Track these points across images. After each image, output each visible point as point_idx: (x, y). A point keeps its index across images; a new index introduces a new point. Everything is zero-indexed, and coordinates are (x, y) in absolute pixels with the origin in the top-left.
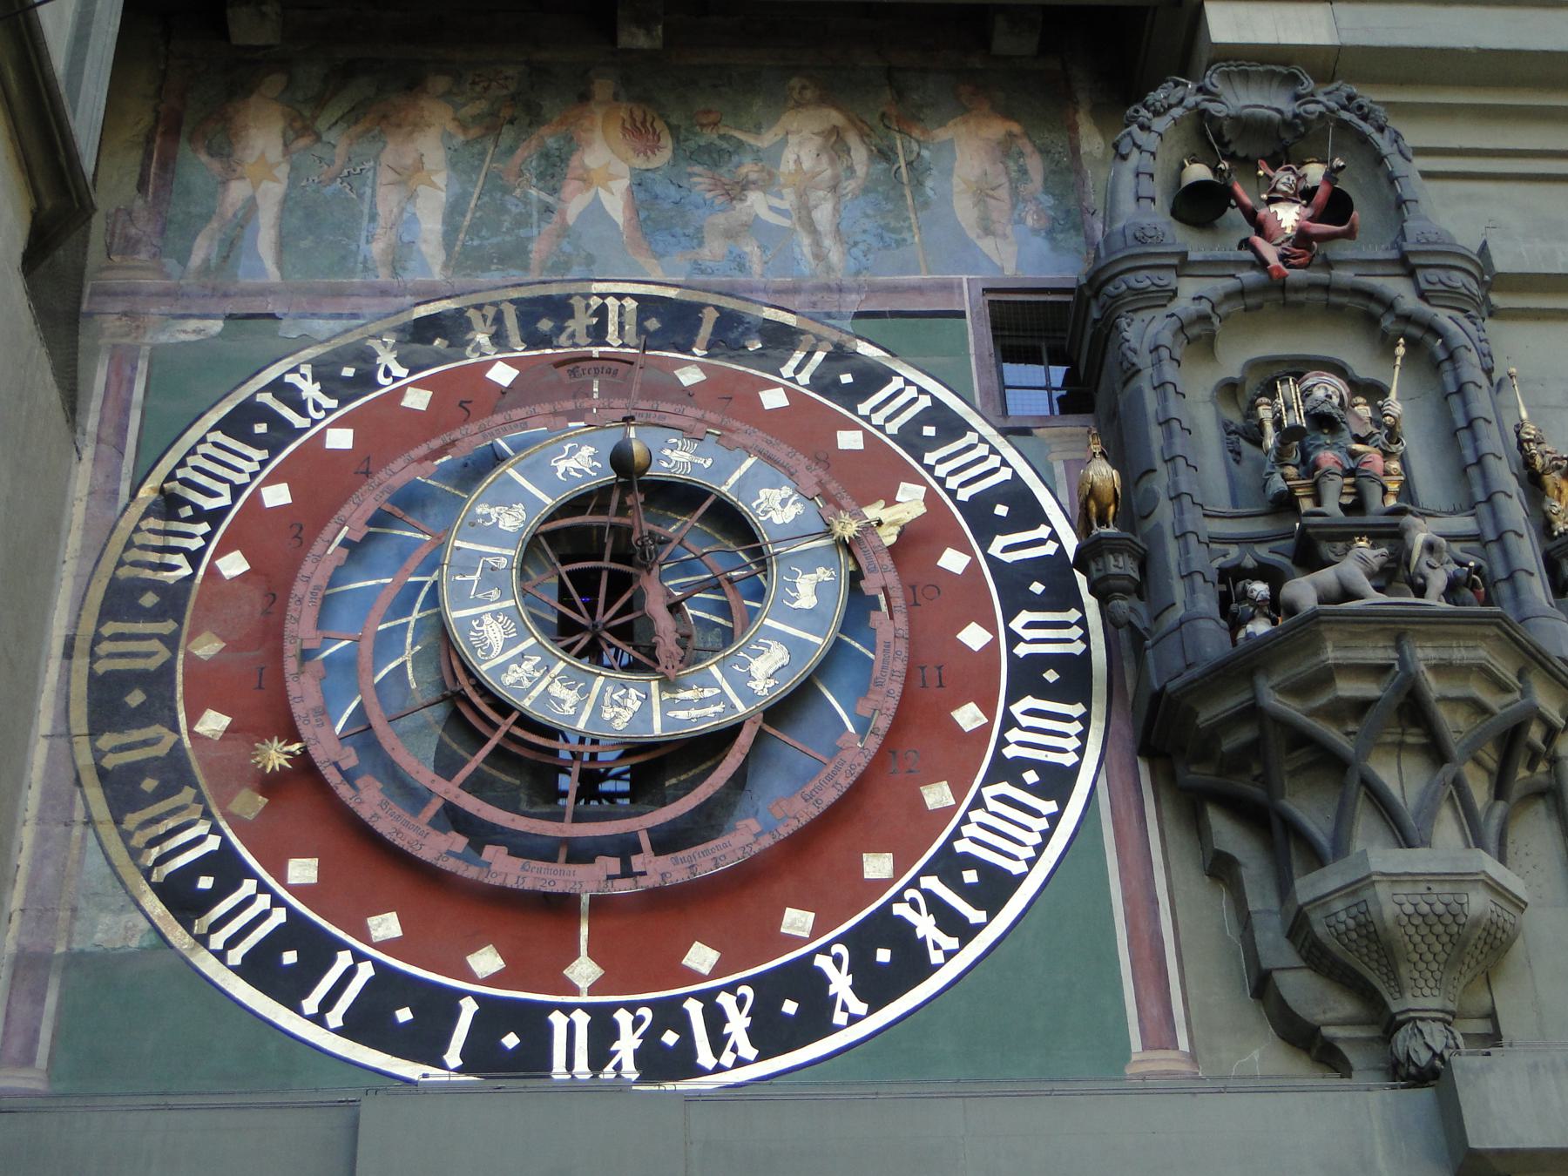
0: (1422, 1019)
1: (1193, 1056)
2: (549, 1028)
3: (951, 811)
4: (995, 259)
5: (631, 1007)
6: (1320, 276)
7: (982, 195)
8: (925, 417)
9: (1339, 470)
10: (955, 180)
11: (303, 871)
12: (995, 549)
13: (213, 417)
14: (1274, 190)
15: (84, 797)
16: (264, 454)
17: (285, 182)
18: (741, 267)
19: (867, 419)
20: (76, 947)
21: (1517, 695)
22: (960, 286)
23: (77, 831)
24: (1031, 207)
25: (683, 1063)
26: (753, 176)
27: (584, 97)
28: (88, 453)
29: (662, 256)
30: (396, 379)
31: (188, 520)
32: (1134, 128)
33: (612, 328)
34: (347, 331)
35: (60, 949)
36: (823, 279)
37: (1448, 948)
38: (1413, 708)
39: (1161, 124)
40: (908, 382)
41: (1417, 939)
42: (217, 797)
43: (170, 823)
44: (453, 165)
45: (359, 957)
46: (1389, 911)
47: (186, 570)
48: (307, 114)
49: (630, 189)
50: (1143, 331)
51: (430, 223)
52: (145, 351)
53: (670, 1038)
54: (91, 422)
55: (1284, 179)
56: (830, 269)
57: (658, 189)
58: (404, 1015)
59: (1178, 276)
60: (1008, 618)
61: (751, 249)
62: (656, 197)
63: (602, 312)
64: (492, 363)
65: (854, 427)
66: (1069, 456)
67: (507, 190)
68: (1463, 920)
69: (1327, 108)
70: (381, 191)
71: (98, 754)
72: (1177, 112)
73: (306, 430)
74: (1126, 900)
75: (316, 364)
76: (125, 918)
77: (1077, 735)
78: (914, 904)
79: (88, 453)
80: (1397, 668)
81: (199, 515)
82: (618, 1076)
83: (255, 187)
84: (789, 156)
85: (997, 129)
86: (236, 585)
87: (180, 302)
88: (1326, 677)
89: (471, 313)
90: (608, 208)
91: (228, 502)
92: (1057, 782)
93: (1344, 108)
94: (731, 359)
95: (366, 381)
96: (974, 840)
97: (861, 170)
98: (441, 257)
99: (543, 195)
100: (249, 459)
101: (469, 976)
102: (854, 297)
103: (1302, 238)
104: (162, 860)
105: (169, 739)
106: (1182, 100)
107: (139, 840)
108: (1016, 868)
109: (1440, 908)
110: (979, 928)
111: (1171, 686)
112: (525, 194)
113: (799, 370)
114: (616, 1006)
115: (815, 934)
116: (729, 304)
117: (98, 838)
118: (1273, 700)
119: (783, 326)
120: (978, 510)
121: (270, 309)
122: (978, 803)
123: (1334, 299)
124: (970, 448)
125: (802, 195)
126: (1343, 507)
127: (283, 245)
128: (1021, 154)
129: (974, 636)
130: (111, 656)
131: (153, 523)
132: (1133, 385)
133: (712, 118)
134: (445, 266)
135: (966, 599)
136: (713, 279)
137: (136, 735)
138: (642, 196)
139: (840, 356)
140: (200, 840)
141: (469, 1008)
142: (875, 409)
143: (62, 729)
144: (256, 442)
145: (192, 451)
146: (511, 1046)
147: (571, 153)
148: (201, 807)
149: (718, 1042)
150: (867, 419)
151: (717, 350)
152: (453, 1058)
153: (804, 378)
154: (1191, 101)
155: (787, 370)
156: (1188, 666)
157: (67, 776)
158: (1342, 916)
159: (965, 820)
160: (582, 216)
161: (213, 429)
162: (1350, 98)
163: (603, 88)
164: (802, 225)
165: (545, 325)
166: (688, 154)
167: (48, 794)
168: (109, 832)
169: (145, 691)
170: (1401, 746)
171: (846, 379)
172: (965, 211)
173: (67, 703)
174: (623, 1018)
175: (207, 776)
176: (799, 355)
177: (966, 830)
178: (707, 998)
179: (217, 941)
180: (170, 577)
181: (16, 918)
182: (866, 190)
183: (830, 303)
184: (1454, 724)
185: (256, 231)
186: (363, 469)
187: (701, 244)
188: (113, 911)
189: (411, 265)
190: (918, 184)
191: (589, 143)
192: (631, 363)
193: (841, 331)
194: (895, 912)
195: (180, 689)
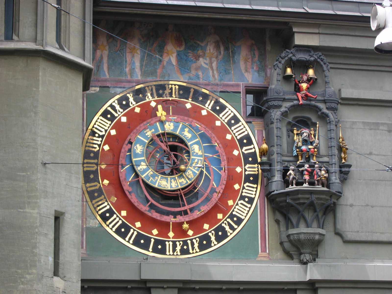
1: (269, 254)
2: (166, 245)
3: (232, 206)
5: (179, 241)
7: (246, 61)
10: (241, 56)
11: (124, 213)
12: (243, 150)
14: (303, 80)
17: (108, 51)
18: (198, 78)
23: (85, 203)
24: (255, 64)
26: (201, 54)
29: (183, 74)
30: (133, 105)
31: (97, 137)
40: (229, 109)
41: (307, 242)
43: (100, 203)
45: (134, 230)
47: (98, 148)
51: (137, 64)
53: (185, 247)
56: (215, 79)
60: (245, 166)
61: (200, 73)
62: (182, 58)
64: (150, 102)
65: (219, 120)
66: (258, 129)
68: (314, 240)
69: (315, 58)
70: (127, 54)
75: (118, 100)
76: (94, 221)
77: (255, 191)
78: (226, 224)
80: (310, 199)
81: (99, 136)
83: (102, 52)
84: (208, 48)
89: (146, 88)
92: (251, 200)
93: (318, 58)
94: (196, 102)
95: (128, 105)
97: (222, 53)
98: (140, 73)
99: (159, 57)
101: (152, 234)
105: (99, 185)
106: (288, 55)
107: (95, 206)
109: (311, 238)
110: (236, 229)
111: (273, 193)
113: (209, 105)
114: (176, 241)
115: (209, 228)
116: (196, 88)
117: (88, 205)
120: (240, 141)
121: (108, 85)
122: (237, 204)
123: (310, 107)
124: (240, 126)
125: (210, 59)
127: (109, 69)
129: (238, 170)
130: (87, 167)
131: (90, 137)
132: (272, 125)
134: (141, 75)
136: (193, 81)
139: (217, 102)
140: (106, 206)
141: (153, 240)
145: (97, 121)
147: (165, 45)
148: (105, 199)
149: (193, 248)
152: (151, 249)
155: (207, 105)
156: (277, 190)
158: (296, 237)
159: (235, 208)
164: (210, 67)
174: (178, 243)
175: (106, 193)
176: (209, 102)
177: (236, 210)
178: (191, 240)
179: (111, 226)
180: (96, 150)
183: (215, 88)
185: (103, 64)
186: (129, 127)
187: (190, 71)
188: (92, 219)
189: (135, 75)
190: (233, 57)
192: (177, 102)
193: (217, 95)
195: (99, 175)
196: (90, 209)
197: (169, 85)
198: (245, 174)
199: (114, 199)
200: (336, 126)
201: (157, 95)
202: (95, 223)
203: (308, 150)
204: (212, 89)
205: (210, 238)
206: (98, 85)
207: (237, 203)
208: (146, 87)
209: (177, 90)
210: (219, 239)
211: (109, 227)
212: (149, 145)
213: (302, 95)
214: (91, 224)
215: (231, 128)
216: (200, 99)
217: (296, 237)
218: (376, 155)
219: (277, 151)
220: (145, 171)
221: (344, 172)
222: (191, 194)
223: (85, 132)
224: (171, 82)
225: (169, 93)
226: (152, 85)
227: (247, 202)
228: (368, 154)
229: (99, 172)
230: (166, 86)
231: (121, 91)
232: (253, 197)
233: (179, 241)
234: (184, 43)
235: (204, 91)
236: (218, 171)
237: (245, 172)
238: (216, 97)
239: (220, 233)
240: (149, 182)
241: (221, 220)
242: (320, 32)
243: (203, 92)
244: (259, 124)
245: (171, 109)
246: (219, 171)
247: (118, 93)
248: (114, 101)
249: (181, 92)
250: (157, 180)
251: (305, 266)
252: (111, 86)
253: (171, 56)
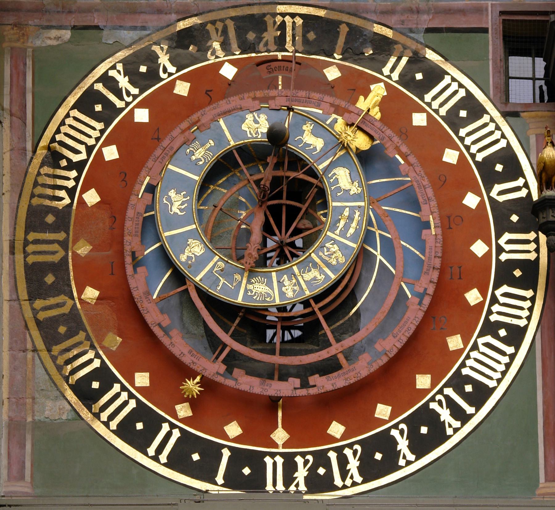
2: (265, 464)
3: (460, 352)
5: (303, 455)
11: (142, 379)
12: (493, 194)
13: (72, 100)
22: (487, 10)
30: (170, 74)
31: (65, 168)
33: (289, 39)
34: (140, 39)
35: (29, 419)
40: (453, 79)
42: (96, 336)
43: (75, 352)
45: (173, 426)
47: (67, 201)
52: (29, 52)
53: (321, 471)
60: (498, 237)
64: (221, 64)
65: (421, 110)
71: (35, 312)
73: (122, 109)
74: (544, 403)
75: (124, 61)
76: (58, 403)
81: (71, 166)
86: (94, 210)
89: (209, 27)
91: (85, 157)
92: (515, 336)
94: (355, 62)
95: (153, 76)
96: (472, 368)
100: (94, 129)
101: (225, 436)
102: (425, 17)
105: (70, 303)
107: (60, 361)
110: (472, 416)
113: (393, 69)
114: (296, 454)
115: (392, 418)
117: (40, 359)
119: (384, 38)
120: (485, 167)
121: (96, 22)
122: (475, 347)
124: (485, 125)
129: (479, 248)
130: (34, 253)
131: (46, 170)
135: (475, 225)
137: (52, 301)
139: (417, 60)
140: (90, 361)
141: (226, 453)
142: (434, 98)
143: (14, 297)
145: (63, 123)
146: (247, 474)
148: (89, 343)
149: (344, 473)
150: (429, 104)
151: (347, 55)
152: (220, 479)
153: (395, 76)
155: (386, 70)
161: (72, 108)
165: (251, 36)
167: (13, 333)
168: (44, 354)
169: (54, 275)
171: (419, 76)
173: (16, 281)
174: (299, 460)
175: (90, 325)
176: (393, 60)
178: (339, 450)
179: (104, 416)
180: (61, 205)
181: (6, 402)
193: (417, 41)
194: (431, 407)
195: (72, 274)
196: (46, 370)
197: (274, 15)
198: (498, 260)
199: (114, 341)
201: (239, 47)
202: (60, 409)
204: (403, 22)
205: (395, 443)
206: (68, 24)
207: (476, 343)
208: (209, 25)
209: (299, 31)
210: (420, 447)
211: (99, 419)
212: (218, 188)
214: (47, 412)
215: (457, 133)
216: (366, 54)
220: (201, 262)
222: (338, 321)
223: (29, 154)
224: (281, 9)
225: (275, 38)
226: (226, 19)
227: (503, 340)
229: (71, 267)
230: (265, 19)
231: (136, 38)
232: (522, 325)
233: (303, 455)
235: (378, 29)
236: (418, 253)
237: (498, 254)
238: (414, 47)
239: (424, 430)
240: (216, 292)
243: (376, 34)
244: (541, 117)
245: (280, 83)
246: (421, 253)
247: (127, 44)
248: (112, 66)
249: (311, 36)
250: (241, 282)
252: (105, 24)
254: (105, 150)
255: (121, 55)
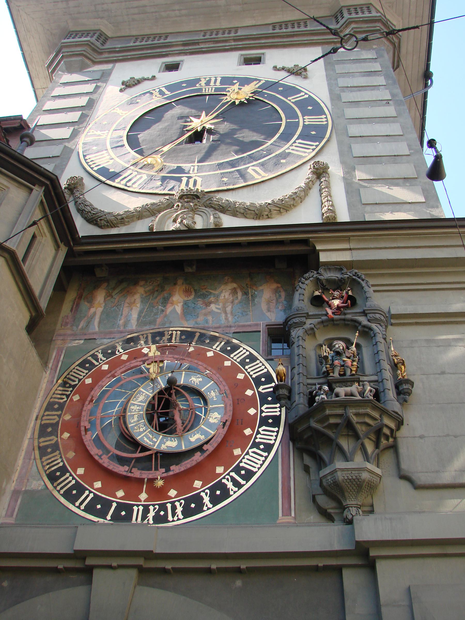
0: (352, 507)
1: (295, 518)
4: (270, 318)
5: (154, 505)
6: (343, 317)
7: (269, 302)
8: (247, 357)
9: (339, 365)
10: (263, 299)
11: (81, 471)
12: (260, 389)
13: (77, 363)
14: (334, 296)
15: (34, 453)
16: (87, 371)
19: (232, 358)
20: (27, 489)
21: (379, 421)
22: (260, 324)
23: (31, 462)
25: (164, 519)
26: (213, 300)
27: (175, 284)
28: (48, 372)
32: (300, 283)
33: (173, 338)
34: (112, 341)
35: (23, 489)
36: (226, 324)
37: (357, 488)
38: (349, 425)
39: (307, 282)
40: (244, 349)
43: (53, 459)
44: (142, 302)
46: (341, 478)
48: (111, 292)
49: (183, 306)
50: (295, 333)
51: (134, 315)
52: (65, 348)
54: (50, 365)
55: (336, 293)
56: (228, 322)
57: (190, 305)
58: (99, 506)
59: (306, 319)
60: (261, 407)
61: (210, 318)
62: (189, 307)
63: (172, 334)
65: (228, 360)
67: (154, 307)
68: (360, 480)
70: (125, 308)
71: (39, 443)
72: (311, 279)
75: (102, 350)
76: (39, 482)
79: (48, 372)
82: (148, 523)
83: (97, 309)
84: (222, 295)
85: (274, 286)
87: (75, 336)
88: (327, 417)
89: (141, 336)
90: (177, 309)
92: (268, 448)
93: (354, 275)
94: (201, 345)
95: (114, 353)
96: (245, 463)
98: (136, 323)
101: (115, 497)
102: (233, 328)
103: (338, 308)
104: (49, 468)
105: (56, 439)
107: (45, 464)
108: (255, 470)
109: (354, 477)
110: (244, 485)
112: (158, 308)
114: (150, 505)
115: (202, 487)
118: (313, 424)
119: (215, 336)
122: (248, 453)
123: (346, 322)
126: (340, 375)
127: (100, 323)
128: (280, 292)
129: (252, 411)
130: (46, 420)
131: (60, 388)
133: (205, 287)
134: (136, 326)
136: (200, 325)
137: (48, 438)
138: (185, 306)
139: (228, 343)
140: (59, 463)
141: (114, 505)
143: (32, 437)
144: (86, 369)
145: (71, 371)
146: (123, 514)
147: (170, 297)
148: (60, 456)
149: (174, 514)
150: (232, 358)
151: (198, 343)
152: (109, 517)
153: (218, 349)
154: (315, 276)
155: (214, 347)
157: (31, 448)
158: (330, 480)
159: (244, 458)
160: (171, 312)
162: (356, 273)
163: (180, 282)
166: (197, 296)
167: (27, 452)
168: (39, 461)
170: (348, 435)
171: (229, 348)
172: (264, 306)
174: (151, 508)
175: (63, 448)
176: (218, 343)
177: (243, 460)
178: (173, 503)
179: (58, 488)
180: (62, 401)
181: (15, 482)
182: (240, 302)
183: (227, 330)
184: (361, 429)
187: (198, 317)
191: (175, 295)
196: (37, 467)
197: (168, 331)
199: (71, 454)
200: (385, 339)
203: (342, 363)
207: (248, 452)
213: (333, 311)
217: (330, 480)
218: (451, 374)
219: (299, 370)
221: (402, 392)
227: (262, 450)
228: (439, 374)
233: (154, 505)
234: (193, 293)
238: (227, 339)
239: (218, 492)
241: (221, 474)
242: (351, 247)
251: (349, 526)
253: (176, 306)
254: (86, 380)
255: (101, 347)
